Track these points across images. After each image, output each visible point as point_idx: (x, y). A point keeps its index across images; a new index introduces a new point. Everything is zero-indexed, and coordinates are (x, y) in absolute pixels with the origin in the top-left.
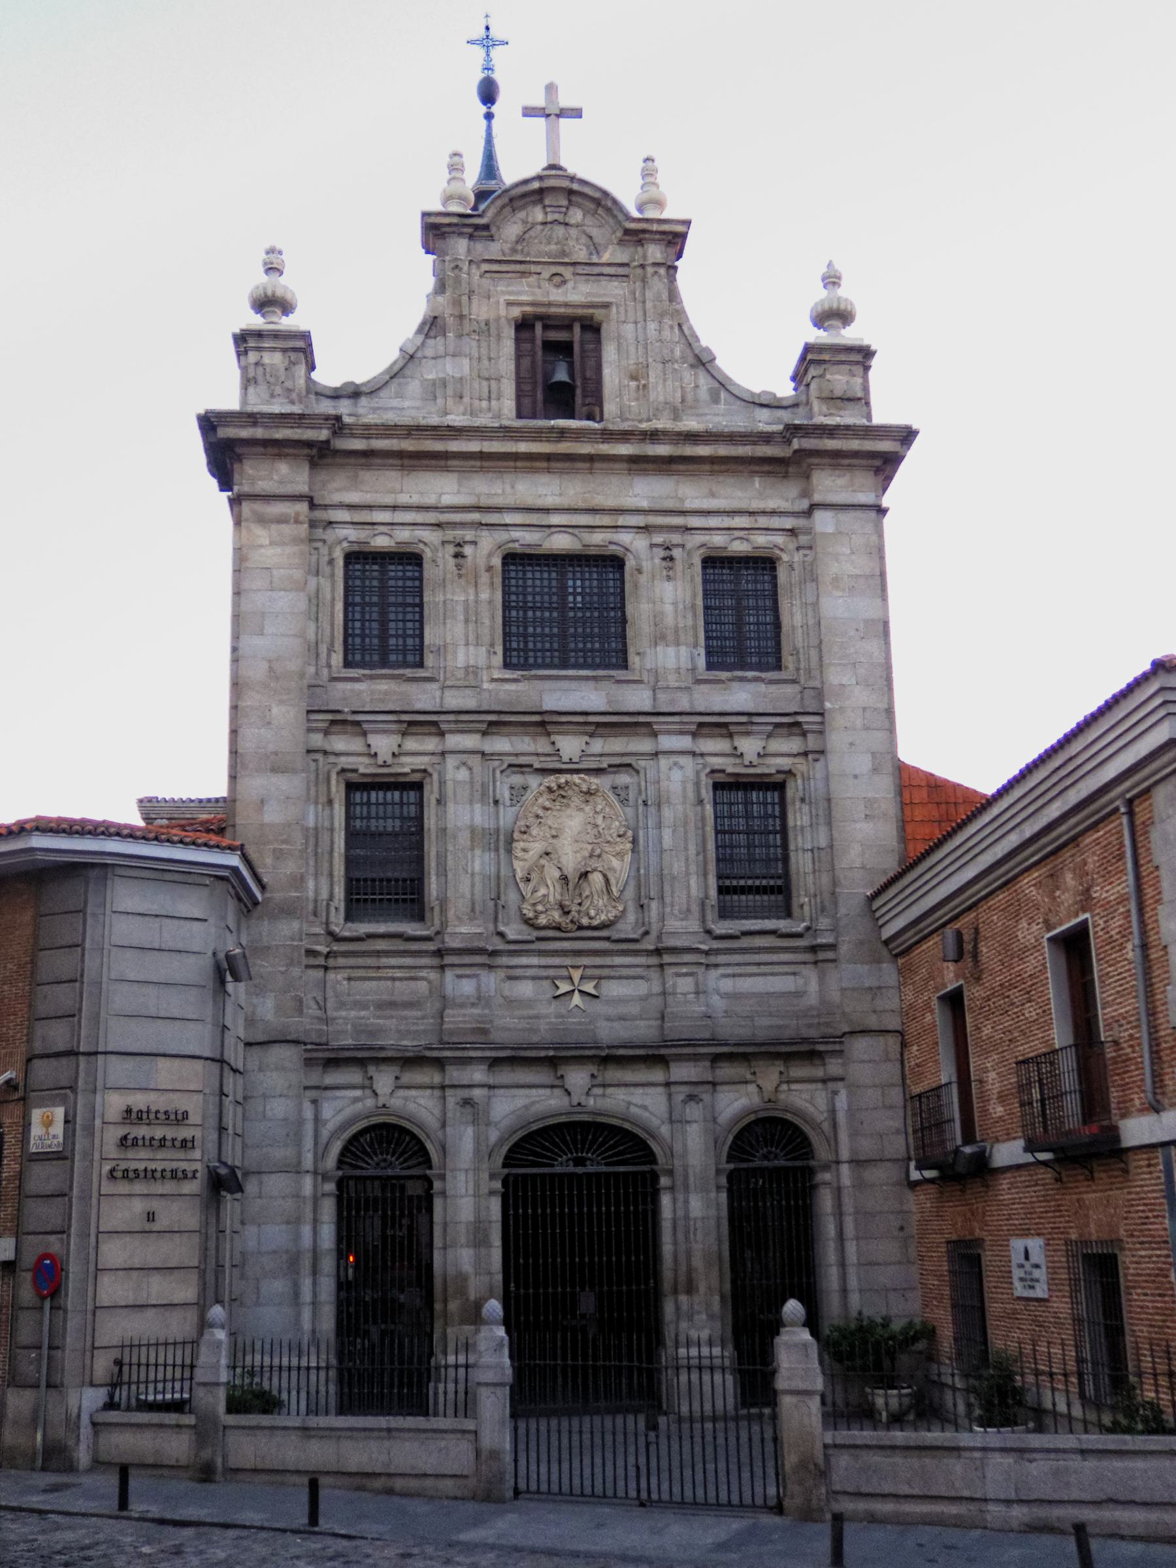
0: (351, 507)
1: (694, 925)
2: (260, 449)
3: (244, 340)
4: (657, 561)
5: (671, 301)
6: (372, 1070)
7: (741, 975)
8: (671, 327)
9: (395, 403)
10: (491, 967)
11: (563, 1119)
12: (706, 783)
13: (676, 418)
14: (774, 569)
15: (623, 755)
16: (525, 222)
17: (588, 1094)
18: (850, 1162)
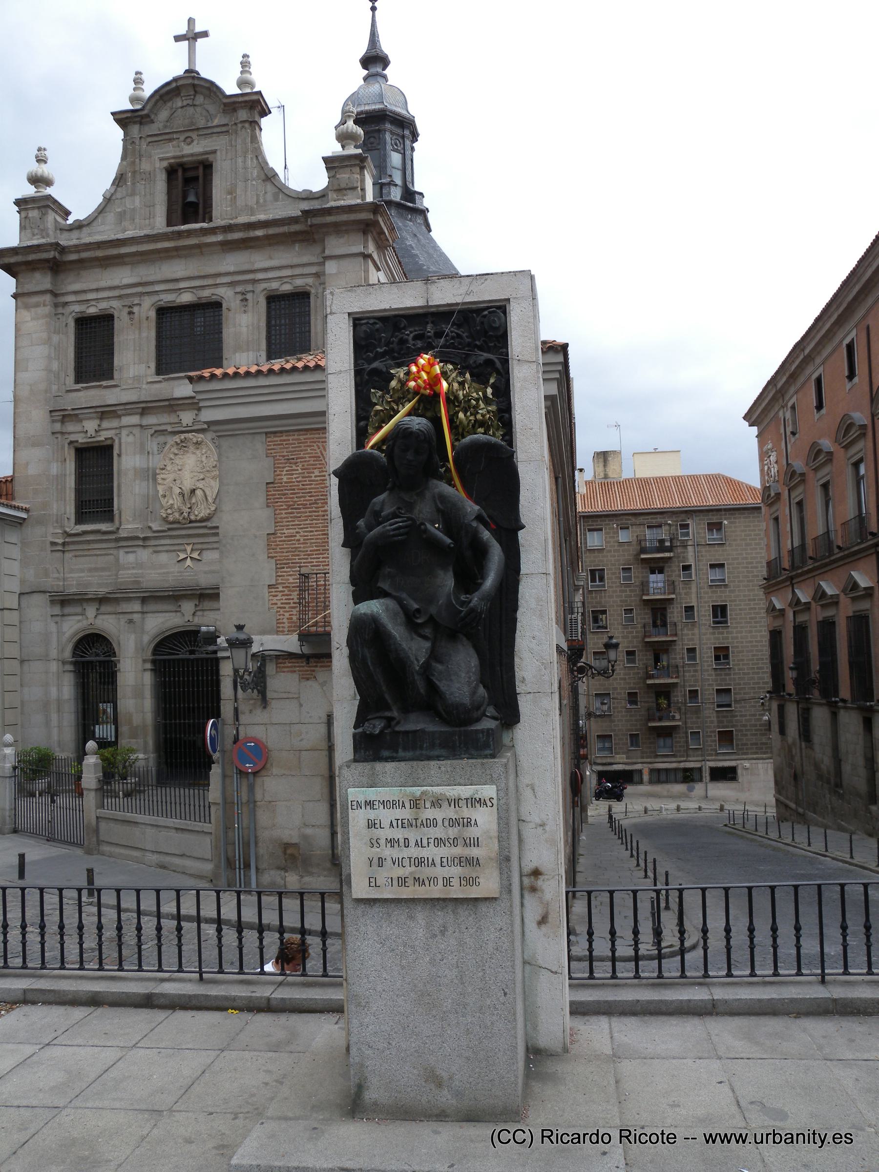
0: (75, 293)
2: (23, 267)
4: (238, 302)
6: (85, 605)
8: (252, 159)
10: (144, 547)
16: (172, 108)
17: (194, 614)
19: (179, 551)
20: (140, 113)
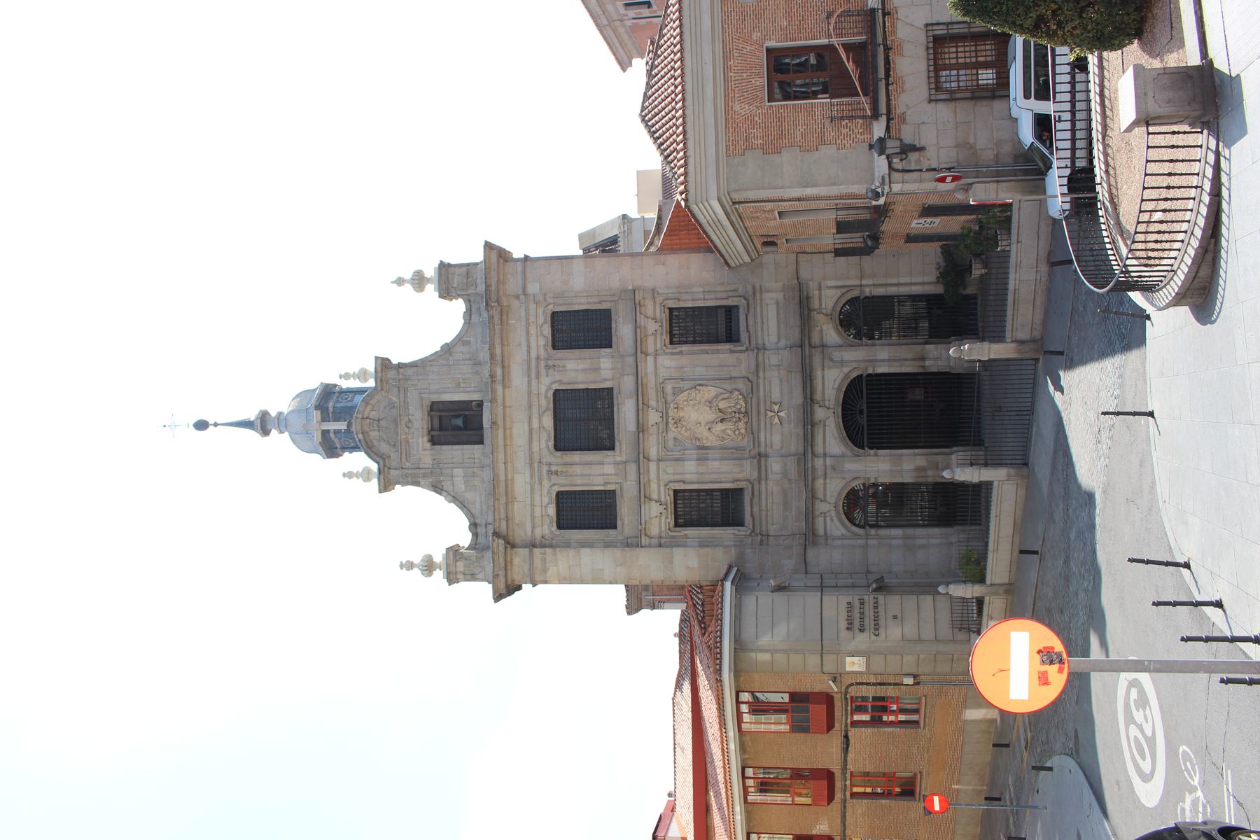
0: (533, 527)
1: (743, 356)
2: (509, 572)
3: (452, 578)
5: (417, 366)
6: (817, 513)
7: (768, 332)
8: (431, 366)
9: (478, 504)
11: (841, 420)
12: (671, 349)
13: (479, 364)
14: (557, 312)
15: (657, 391)
16: (379, 441)
17: (829, 409)
18: (861, 280)
19: (771, 424)
20: (382, 467)
